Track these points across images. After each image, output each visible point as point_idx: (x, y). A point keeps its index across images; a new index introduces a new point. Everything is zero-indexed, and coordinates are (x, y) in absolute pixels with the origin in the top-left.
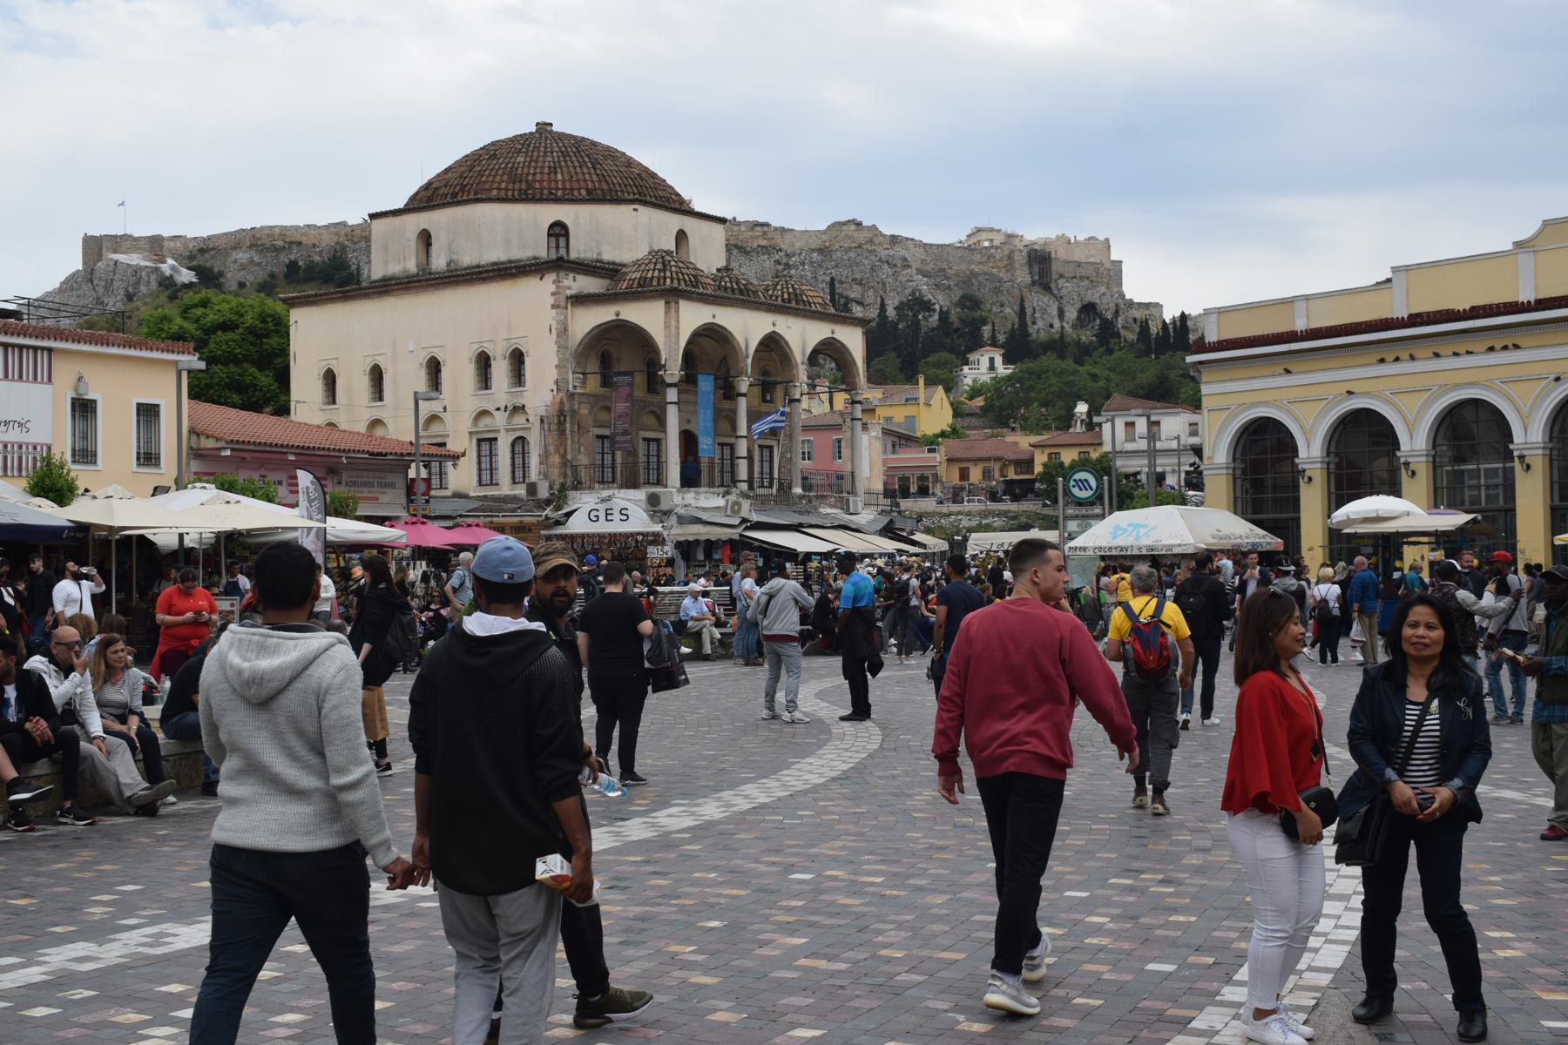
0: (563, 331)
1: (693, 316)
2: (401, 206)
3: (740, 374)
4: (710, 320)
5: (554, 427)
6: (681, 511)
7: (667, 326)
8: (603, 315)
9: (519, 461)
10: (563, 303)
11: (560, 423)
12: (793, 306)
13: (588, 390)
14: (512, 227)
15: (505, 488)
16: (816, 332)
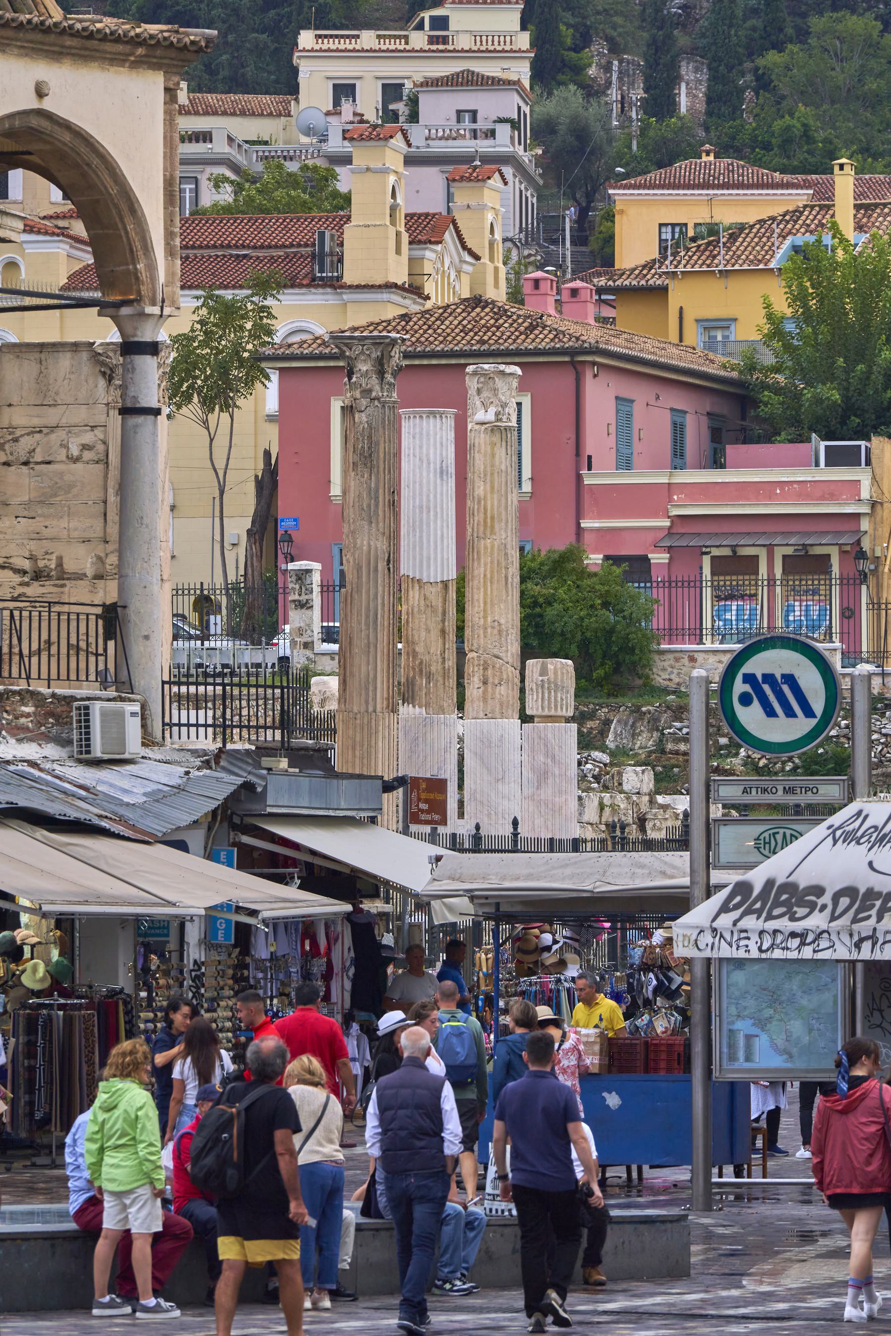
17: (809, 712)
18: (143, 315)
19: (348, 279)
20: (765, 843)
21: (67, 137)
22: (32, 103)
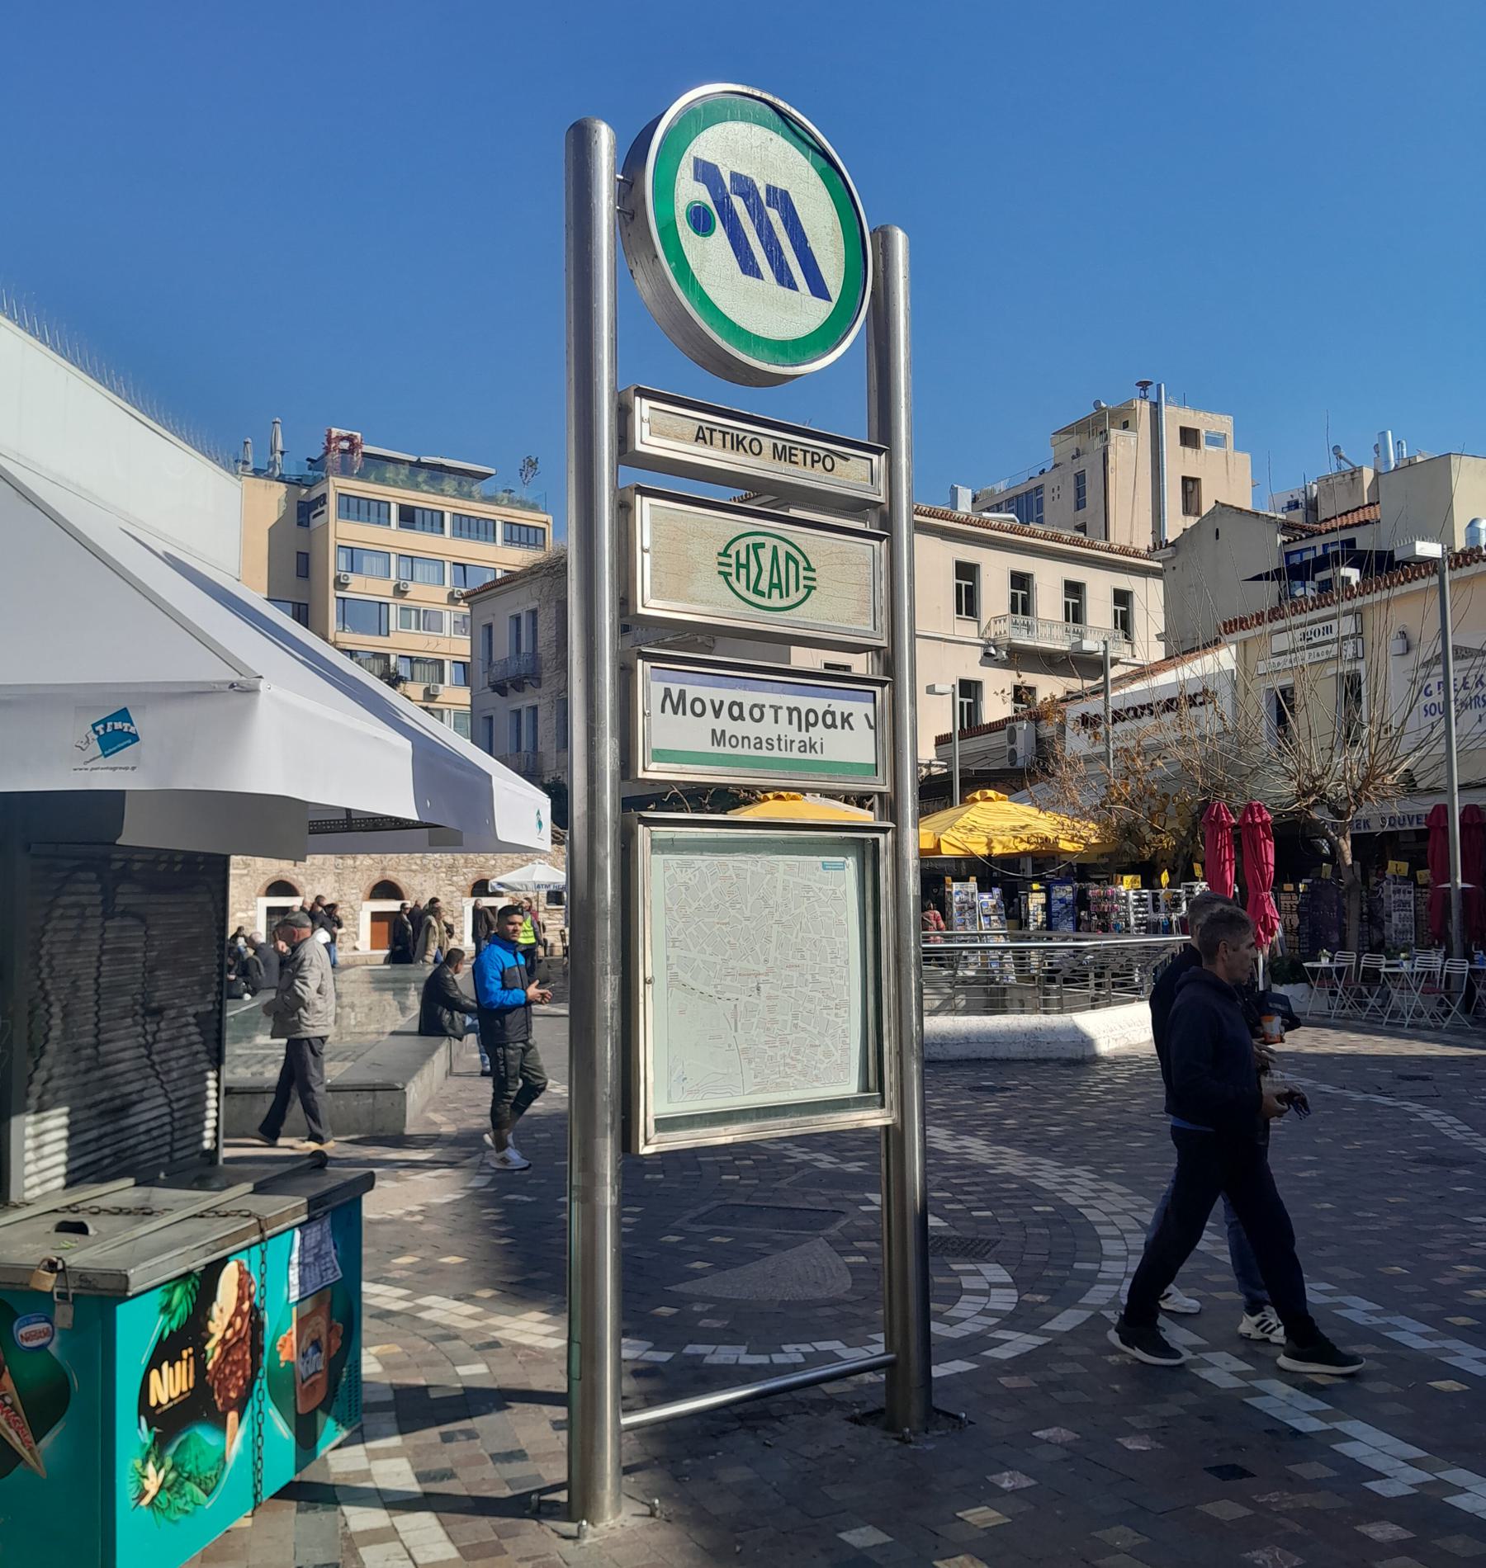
17: (818, 289)
20: (739, 565)
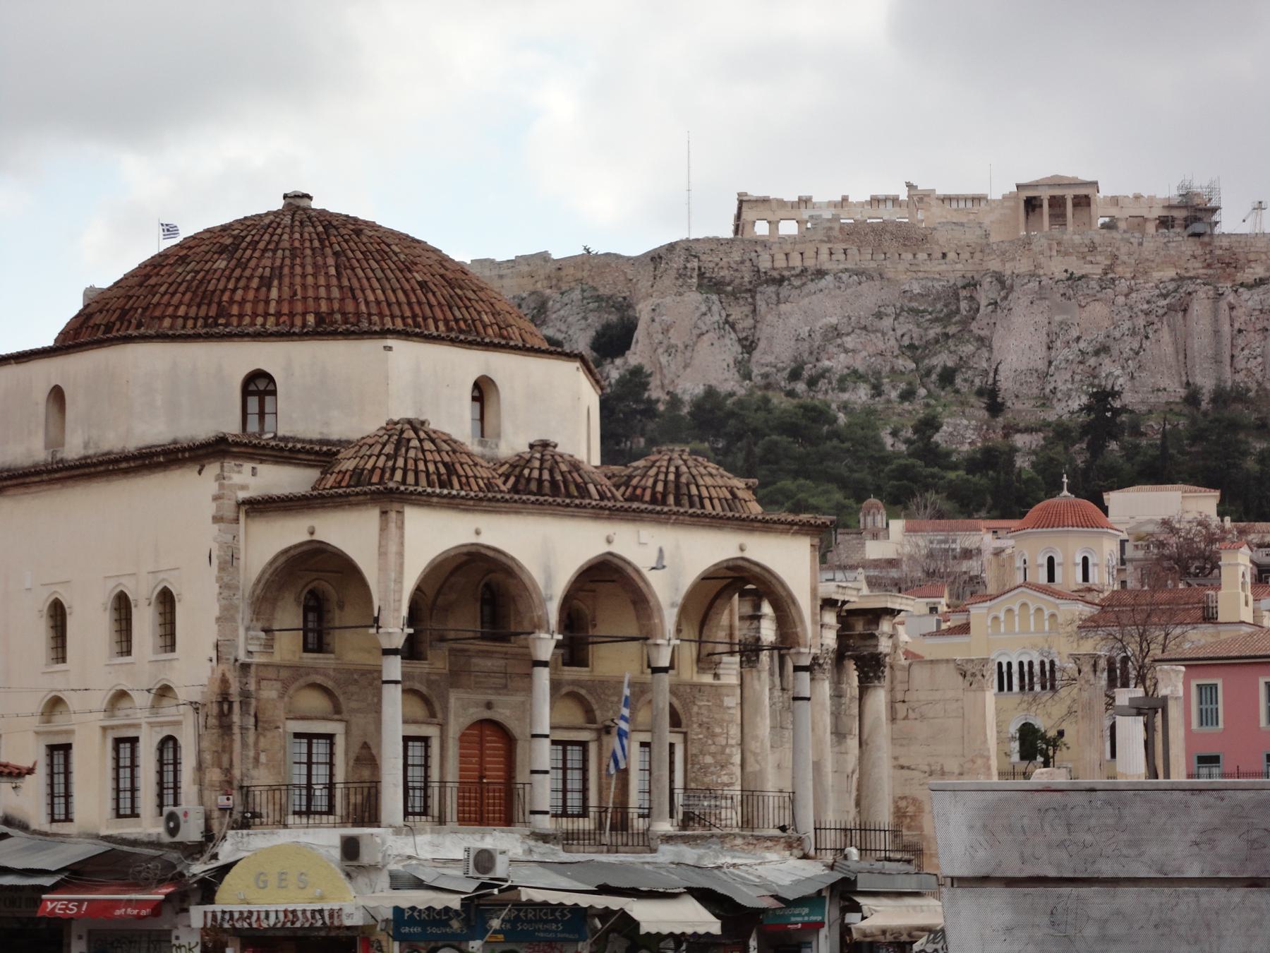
0: (230, 561)
1: (431, 535)
2: (49, 342)
3: (540, 624)
4: (474, 539)
5: (213, 721)
6: (394, 867)
7: (382, 553)
8: (288, 533)
9: (169, 777)
10: (229, 513)
11: (221, 710)
12: (673, 504)
13: (277, 658)
14: (183, 384)
15: (149, 826)
16: (702, 550)
18: (799, 653)
19: (1220, 619)
21: (758, 569)
22: (739, 554)
